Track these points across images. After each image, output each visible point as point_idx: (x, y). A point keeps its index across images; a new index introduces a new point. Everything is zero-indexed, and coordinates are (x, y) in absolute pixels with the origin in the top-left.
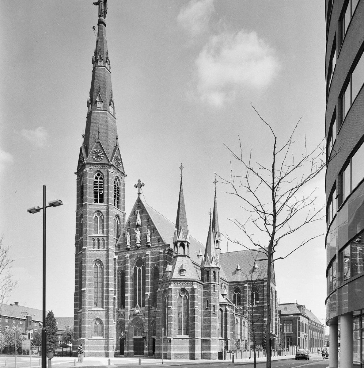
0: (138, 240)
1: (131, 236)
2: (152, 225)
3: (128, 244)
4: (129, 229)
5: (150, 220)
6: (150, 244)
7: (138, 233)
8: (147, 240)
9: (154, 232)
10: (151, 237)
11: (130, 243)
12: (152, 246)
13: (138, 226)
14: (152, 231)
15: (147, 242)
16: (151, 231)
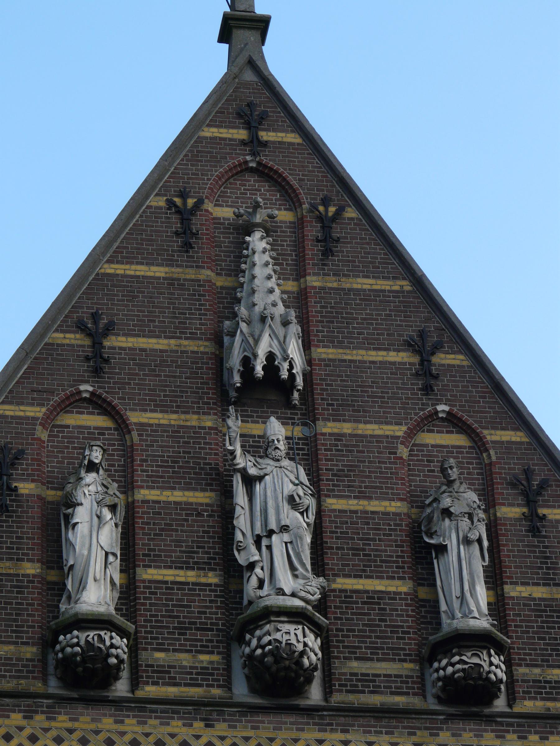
0: (285, 577)
1: (130, 508)
2: (493, 436)
3: (96, 596)
4: (98, 404)
5: (442, 359)
6: (495, 666)
7: (277, 495)
8: (428, 610)
9: (534, 523)
10: (495, 578)
11: (129, 594)
12: (528, 706)
13: (267, 389)
14: (510, 512)
15: (449, 625)
16: (490, 501)
